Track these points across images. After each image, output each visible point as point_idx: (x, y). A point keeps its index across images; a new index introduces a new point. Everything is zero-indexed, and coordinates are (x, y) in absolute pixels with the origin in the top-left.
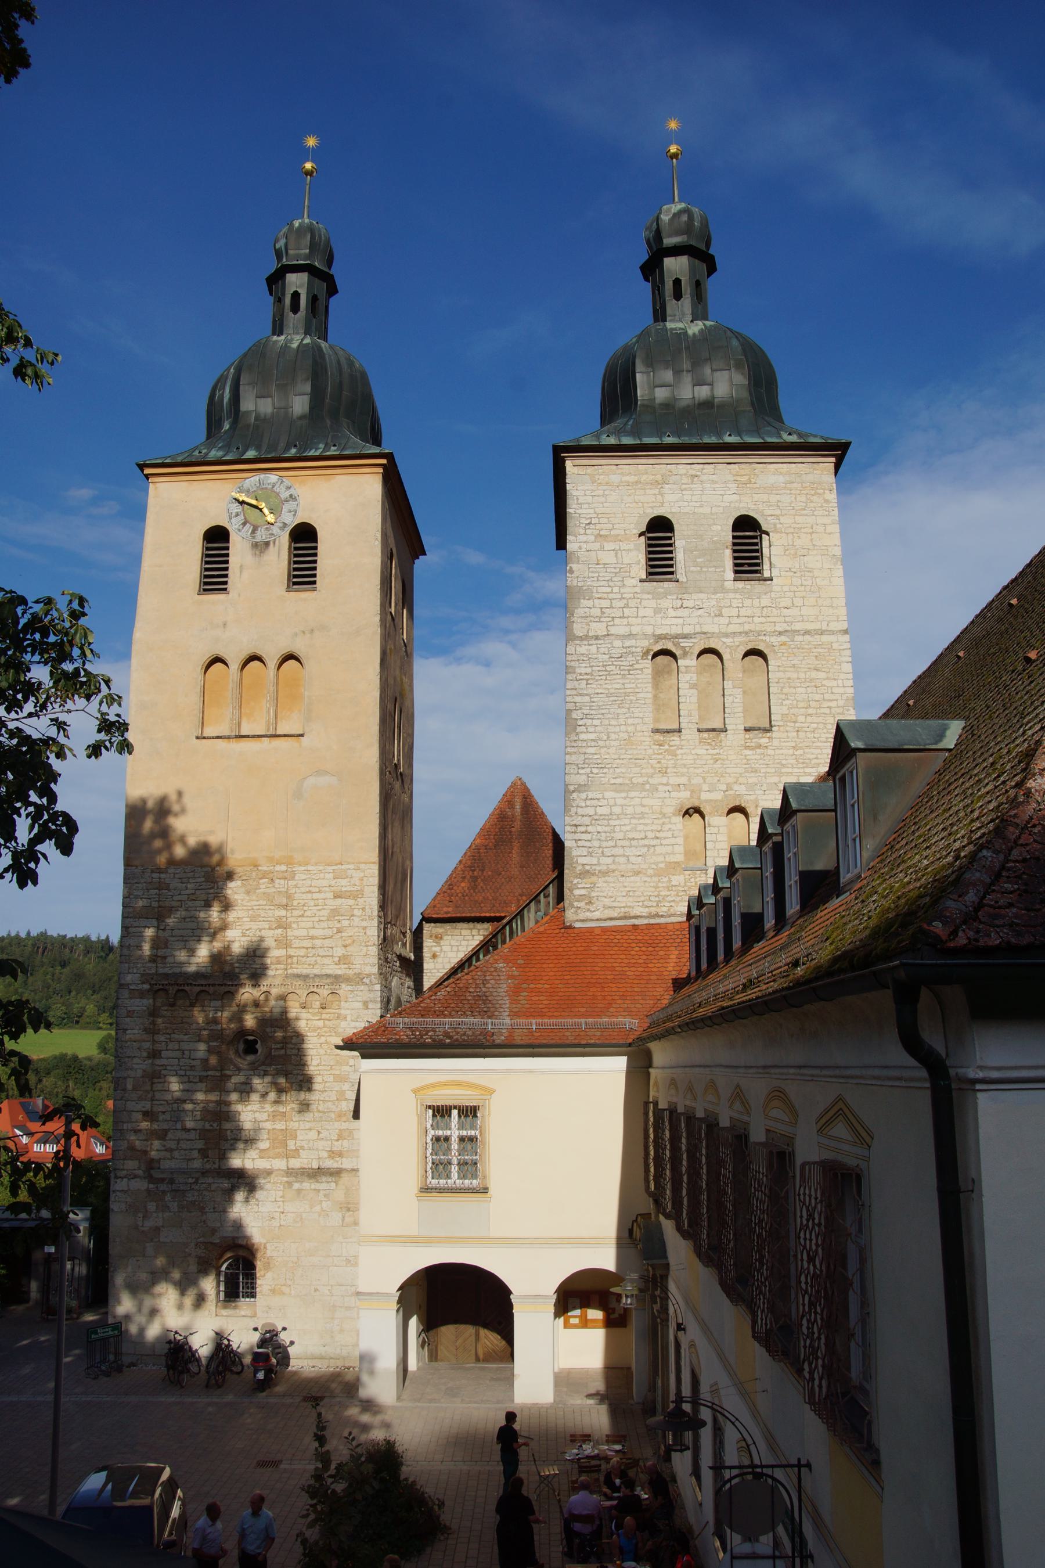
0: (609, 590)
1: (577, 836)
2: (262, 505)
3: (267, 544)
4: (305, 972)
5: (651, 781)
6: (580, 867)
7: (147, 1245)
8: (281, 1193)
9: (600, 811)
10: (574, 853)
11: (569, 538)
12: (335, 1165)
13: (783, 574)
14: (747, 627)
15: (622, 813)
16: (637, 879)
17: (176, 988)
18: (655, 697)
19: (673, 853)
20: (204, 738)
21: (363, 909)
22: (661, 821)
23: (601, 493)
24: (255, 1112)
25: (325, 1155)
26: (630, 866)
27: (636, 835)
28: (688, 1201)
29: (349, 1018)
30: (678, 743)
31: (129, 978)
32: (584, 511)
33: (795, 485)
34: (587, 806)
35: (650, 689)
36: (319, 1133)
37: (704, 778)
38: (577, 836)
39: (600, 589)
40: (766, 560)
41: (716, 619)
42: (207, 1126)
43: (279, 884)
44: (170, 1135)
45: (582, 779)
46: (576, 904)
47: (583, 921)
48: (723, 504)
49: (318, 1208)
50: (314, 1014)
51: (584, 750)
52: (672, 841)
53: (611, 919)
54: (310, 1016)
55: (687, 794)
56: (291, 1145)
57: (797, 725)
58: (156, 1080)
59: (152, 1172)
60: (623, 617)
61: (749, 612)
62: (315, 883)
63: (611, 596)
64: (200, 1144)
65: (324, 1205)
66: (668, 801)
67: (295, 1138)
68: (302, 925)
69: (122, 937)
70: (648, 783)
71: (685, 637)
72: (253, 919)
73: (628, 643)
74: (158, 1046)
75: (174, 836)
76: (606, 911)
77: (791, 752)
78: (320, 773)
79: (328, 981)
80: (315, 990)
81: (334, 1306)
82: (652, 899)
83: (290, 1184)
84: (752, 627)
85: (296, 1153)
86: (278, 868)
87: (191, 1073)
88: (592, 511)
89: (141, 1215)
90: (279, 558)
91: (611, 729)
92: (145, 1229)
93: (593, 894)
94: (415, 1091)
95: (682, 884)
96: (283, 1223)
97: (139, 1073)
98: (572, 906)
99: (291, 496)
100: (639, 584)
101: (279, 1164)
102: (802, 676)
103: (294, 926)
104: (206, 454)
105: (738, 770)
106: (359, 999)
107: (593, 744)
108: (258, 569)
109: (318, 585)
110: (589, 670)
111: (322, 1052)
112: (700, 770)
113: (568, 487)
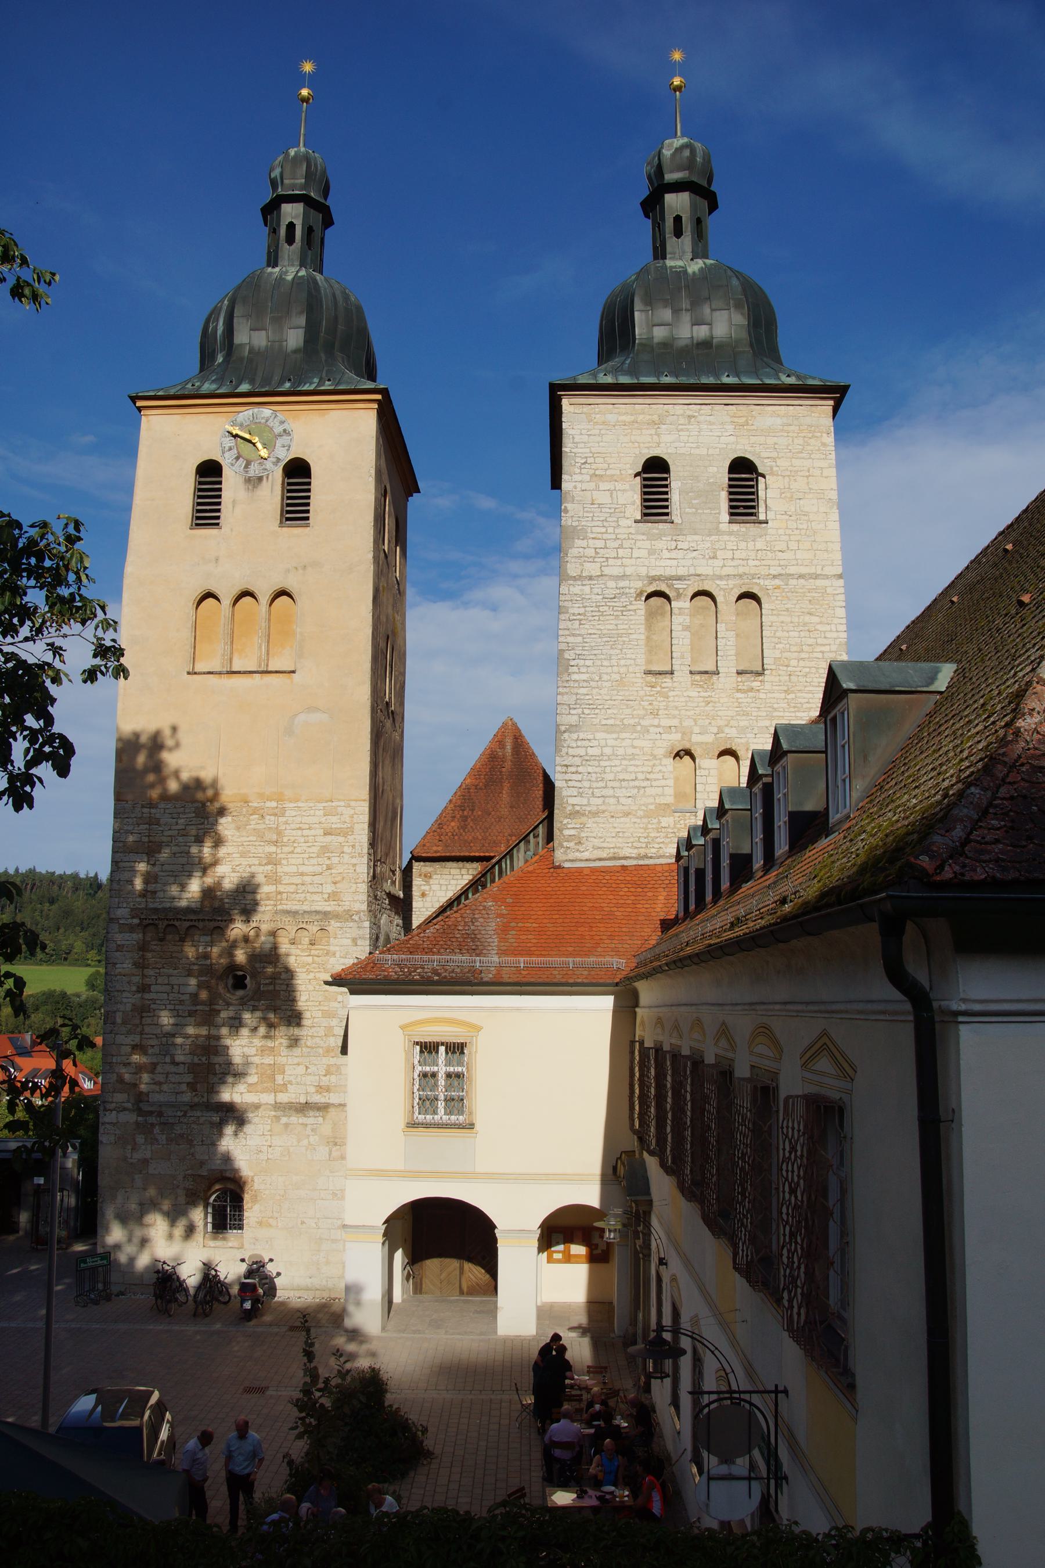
0: (604, 530)
1: (568, 777)
2: (256, 440)
3: (260, 479)
4: (294, 908)
5: (643, 723)
6: (570, 808)
7: (136, 1176)
8: (268, 1127)
9: (590, 751)
10: (564, 793)
11: (564, 476)
12: (323, 1100)
13: (778, 517)
14: (741, 570)
15: (613, 754)
16: (627, 820)
17: (166, 923)
18: (648, 638)
19: (663, 795)
20: (195, 673)
21: (353, 846)
22: (651, 763)
23: (597, 432)
25: (312, 1089)
26: (620, 807)
28: (672, 1138)
29: (338, 955)
30: (670, 685)
31: (120, 913)
32: (580, 450)
33: (792, 428)
34: (578, 747)
35: (642, 630)
36: (307, 1068)
37: (695, 720)
38: (568, 777)
39: (595, 530)
40: (761, 503)
41: (711, 561)
42: (196, 1060)
43: (270, 820)
44: (159, 1069)
45: (573, 720)
46: (565, 844)
47: (572, 861)
48: (720, 446)
49: (305, 1142)
50: (303, 950)
51: (576, 690)
52: (663, 783)
53: (600, 859)
54: (298, 952)
55: (679, 736)
56: (279, 1079)
57: (789, 669)
58: (144, 1014)
59: (141, 1105)
60: (617, 558)
61: (744, 555)
62: (305, 820)
63: (605, 536)
64: (189, 1078)
65: (312, 1139)
66: (659, 743)
68: (293, 861)
69: (112, 872)
70: (639, 724)
71: (679, 578)
72: (243, 855)
73: (621, 584)
74: (147, 981)
75: (166, 771)
76: (595, 852)
77: (783, 695)
78: (312, 709)
79: (317, 917)
80: (304, 926)
82: (642, 840)
84: (746, 570)
85: (284, 1088)
86: (269, 804)
87: (180, 1007)
88: (588, 450)
89: (130, 1147)
90: (272, 493)
91: (603, 670)
93: (583, 834)
94: (402, 1027)
95: (672, 825)
96: (270, 1157)
97: (129, 1007)
98: (562, 847)
99: (285, 431)
100: (634, 525)
101: (267, 1098)
102: (796, 620)
103: (284, 862)
104: (200, 387)
105: (730, 713)
106: (348, 935)
107: (585, 684)
108: (251, 504)
109: (311, 521)
110: (582, 611)
111: (311, 988)
112: (692, 712)
113: (564, 426)
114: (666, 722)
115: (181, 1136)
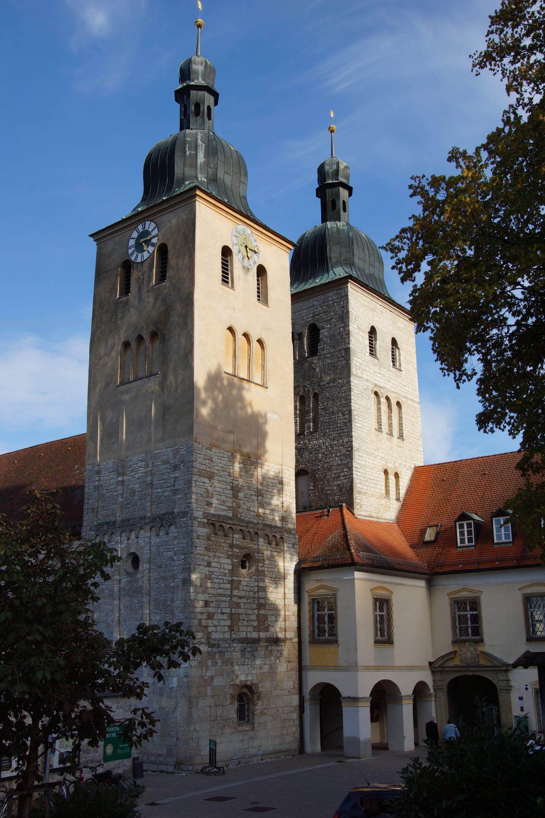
7: (208, 688)
8: (264, 652)
17: (219, 524)
24: (251, 603)
27: (371, 477)
44: (215, 617)
50: (273, 548)
59: (210, 640)
64: (228, 623)
67: (267, 620)
80: (274, 534)
81: (285, 719)
83: (267, 647)
89: (204, 668)
92: (207, 678)
101: (263, 635)
106: (291, 542)
114: (382, 455)
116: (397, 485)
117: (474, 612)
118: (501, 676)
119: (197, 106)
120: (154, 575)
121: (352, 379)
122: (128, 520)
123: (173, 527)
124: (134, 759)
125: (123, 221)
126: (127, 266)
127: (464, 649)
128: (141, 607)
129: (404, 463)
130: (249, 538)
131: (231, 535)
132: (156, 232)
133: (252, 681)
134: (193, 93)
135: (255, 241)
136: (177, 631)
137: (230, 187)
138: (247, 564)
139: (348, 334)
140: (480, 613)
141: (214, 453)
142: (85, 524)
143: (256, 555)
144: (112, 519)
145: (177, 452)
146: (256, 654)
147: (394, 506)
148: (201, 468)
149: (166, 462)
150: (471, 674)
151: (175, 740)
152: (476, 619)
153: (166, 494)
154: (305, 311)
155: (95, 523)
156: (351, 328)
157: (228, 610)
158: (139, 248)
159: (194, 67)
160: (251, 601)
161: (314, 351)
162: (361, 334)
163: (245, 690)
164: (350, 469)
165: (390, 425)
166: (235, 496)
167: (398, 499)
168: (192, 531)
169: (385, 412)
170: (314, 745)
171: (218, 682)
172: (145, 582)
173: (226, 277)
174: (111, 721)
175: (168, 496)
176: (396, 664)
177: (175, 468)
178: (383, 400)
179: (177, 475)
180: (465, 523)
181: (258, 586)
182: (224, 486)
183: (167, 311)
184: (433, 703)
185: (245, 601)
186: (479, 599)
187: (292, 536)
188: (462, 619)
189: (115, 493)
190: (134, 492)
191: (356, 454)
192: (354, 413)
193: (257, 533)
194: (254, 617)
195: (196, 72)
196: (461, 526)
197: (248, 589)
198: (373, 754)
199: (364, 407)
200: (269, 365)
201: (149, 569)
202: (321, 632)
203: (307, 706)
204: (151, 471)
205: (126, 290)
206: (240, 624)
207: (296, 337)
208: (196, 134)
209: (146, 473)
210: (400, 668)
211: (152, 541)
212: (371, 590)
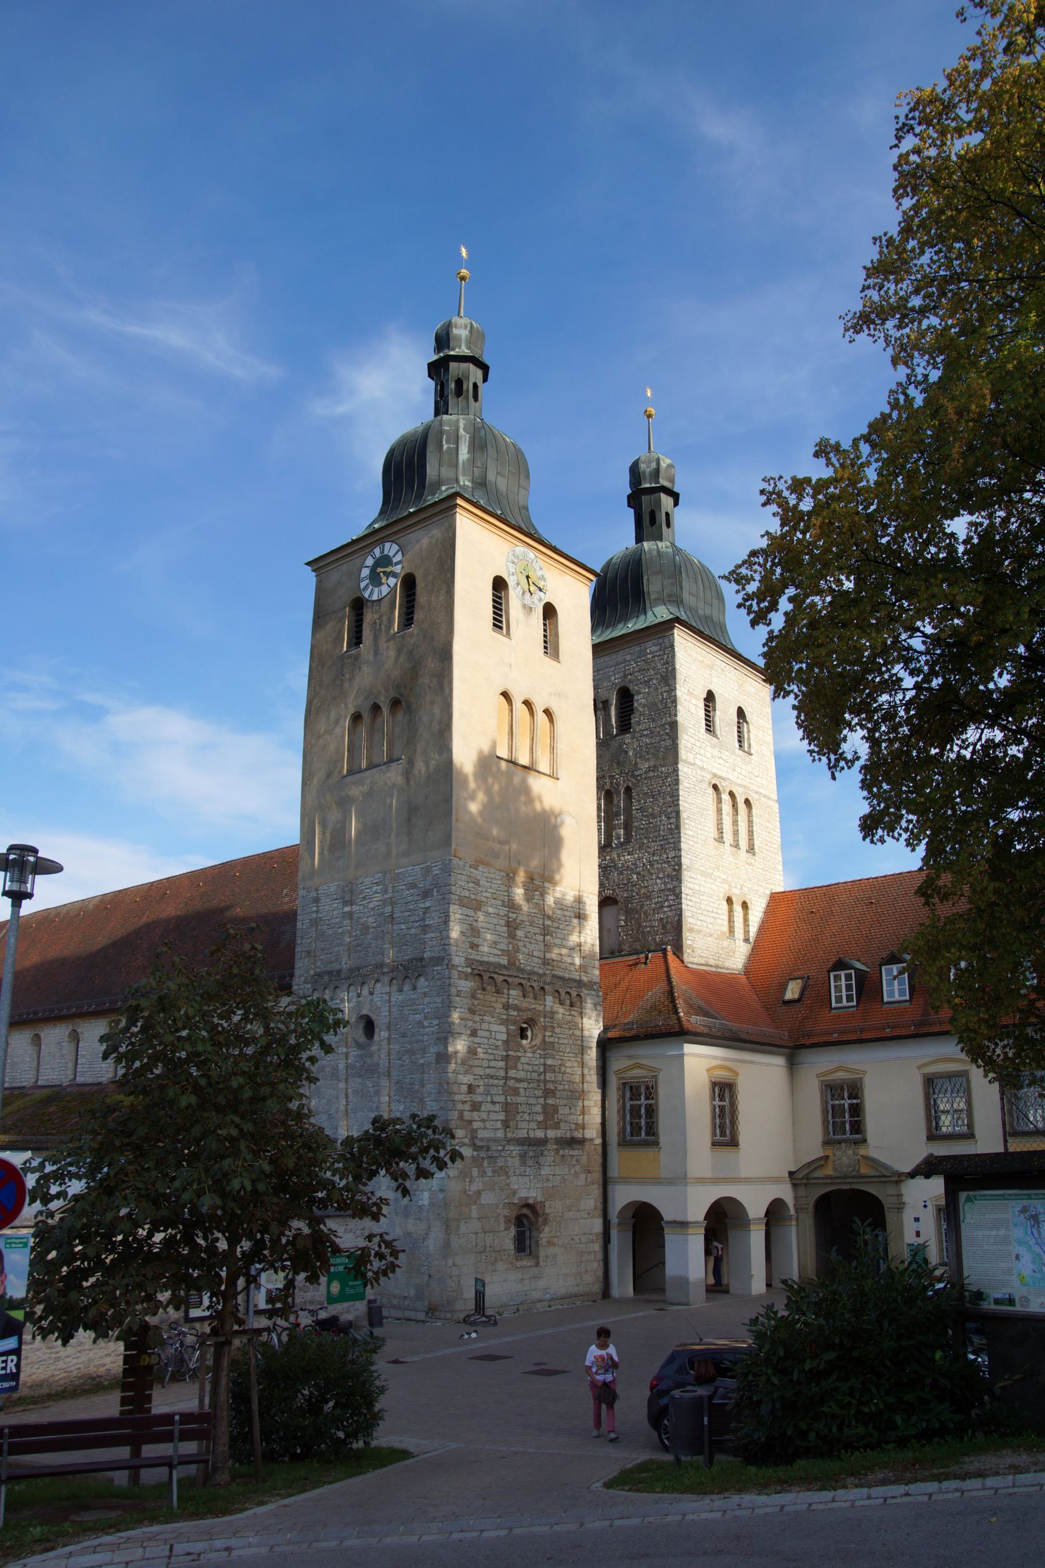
17: (489, 975)
44: (483, 1108)
64: (502, 1116)
83: (557, 1151)
89: (468, 1180)
92: (470, 1193)
101: (551, 1134)
114: (724, 876)
115: (501, 1167)
116: (746, 920)
117: (855, 1101)
118: (891, 1190)
119: (459, 383)
120: (395, 1047)
121: (679, 766)
122: (358, 969)
123: (422, 979)
124: (370, 1302)
125: (353, 542)
126: (359, 605)
127: (839, 1153)
128: (378, 1093)
129: (756, 888)
130: (531, 995)
131: (505, 991)
132: (398, 557)
133: (535, 1198)
134: (453, 365)
135: (541, 569)
136: (428, 1127)
137: (504, 494)
138: (529, 1033)
139: (674, 701)
140: (862, 1101)
141: (481, 872)
142: (297, 973)
143: (542, 1020)
144: (336, 966)
145: (427, 871)
146: (542, 1160)
147: (741, 950)
148: (463, 894)
149: (413, 886)
150: (848, 1187)
151: (426, 1277)
152: (857, 1110)
153: (413, 931)
154: (613, 669)
155: (312, 972)
156: (679, 693)
157: (502, 1099)
158: (375, 579)
159: (455, 331)
160: (534, 1085)
161: (625, 725)
162: (693, 701)
163: (525, 1211)
164: (678, 896)
165: (736, 833)
166: (512, 935)
167: (746, 940)
168: (450, 985)
169: (728, 814)
170: (623, 1286)
171: (487, 1198)
172: (383, 1056)
173: (499, 620)
174: (337, 1250)
175: (416, 935)
176: (742, 1175)
177: (426, 894)
178: (725, 797)
179: (427, 904)
180: (842, 974)
181: (545, 1065)
182: (495, 921)
183: (414, 670)
184: (794, 1229)
185: (525, 1085)
186: (861, 1083)
187: (593, 993)
188: (837, 1111)
189: (340, 930)
190: (366, 928)
191: (686, 875)
192: (684, 815)
193: (543, 988)
194: (538, 1109)
195: (458, 339)
196: (837, 978)
197: (530, 1068)
198: (708, 1299)
199: (697, 807)
200: (561, 746)
201: (389, 1039)
202: (636, 1130)
203: (614, 1233)
204: (391, 898)
205: (357, 639)
206: (519, 1118)
207: (600, 706)
208: (458, 421)
209: (384, 901)
210: (747, 1181)
211: (393, 999)
212: (708, 1071)
